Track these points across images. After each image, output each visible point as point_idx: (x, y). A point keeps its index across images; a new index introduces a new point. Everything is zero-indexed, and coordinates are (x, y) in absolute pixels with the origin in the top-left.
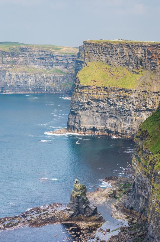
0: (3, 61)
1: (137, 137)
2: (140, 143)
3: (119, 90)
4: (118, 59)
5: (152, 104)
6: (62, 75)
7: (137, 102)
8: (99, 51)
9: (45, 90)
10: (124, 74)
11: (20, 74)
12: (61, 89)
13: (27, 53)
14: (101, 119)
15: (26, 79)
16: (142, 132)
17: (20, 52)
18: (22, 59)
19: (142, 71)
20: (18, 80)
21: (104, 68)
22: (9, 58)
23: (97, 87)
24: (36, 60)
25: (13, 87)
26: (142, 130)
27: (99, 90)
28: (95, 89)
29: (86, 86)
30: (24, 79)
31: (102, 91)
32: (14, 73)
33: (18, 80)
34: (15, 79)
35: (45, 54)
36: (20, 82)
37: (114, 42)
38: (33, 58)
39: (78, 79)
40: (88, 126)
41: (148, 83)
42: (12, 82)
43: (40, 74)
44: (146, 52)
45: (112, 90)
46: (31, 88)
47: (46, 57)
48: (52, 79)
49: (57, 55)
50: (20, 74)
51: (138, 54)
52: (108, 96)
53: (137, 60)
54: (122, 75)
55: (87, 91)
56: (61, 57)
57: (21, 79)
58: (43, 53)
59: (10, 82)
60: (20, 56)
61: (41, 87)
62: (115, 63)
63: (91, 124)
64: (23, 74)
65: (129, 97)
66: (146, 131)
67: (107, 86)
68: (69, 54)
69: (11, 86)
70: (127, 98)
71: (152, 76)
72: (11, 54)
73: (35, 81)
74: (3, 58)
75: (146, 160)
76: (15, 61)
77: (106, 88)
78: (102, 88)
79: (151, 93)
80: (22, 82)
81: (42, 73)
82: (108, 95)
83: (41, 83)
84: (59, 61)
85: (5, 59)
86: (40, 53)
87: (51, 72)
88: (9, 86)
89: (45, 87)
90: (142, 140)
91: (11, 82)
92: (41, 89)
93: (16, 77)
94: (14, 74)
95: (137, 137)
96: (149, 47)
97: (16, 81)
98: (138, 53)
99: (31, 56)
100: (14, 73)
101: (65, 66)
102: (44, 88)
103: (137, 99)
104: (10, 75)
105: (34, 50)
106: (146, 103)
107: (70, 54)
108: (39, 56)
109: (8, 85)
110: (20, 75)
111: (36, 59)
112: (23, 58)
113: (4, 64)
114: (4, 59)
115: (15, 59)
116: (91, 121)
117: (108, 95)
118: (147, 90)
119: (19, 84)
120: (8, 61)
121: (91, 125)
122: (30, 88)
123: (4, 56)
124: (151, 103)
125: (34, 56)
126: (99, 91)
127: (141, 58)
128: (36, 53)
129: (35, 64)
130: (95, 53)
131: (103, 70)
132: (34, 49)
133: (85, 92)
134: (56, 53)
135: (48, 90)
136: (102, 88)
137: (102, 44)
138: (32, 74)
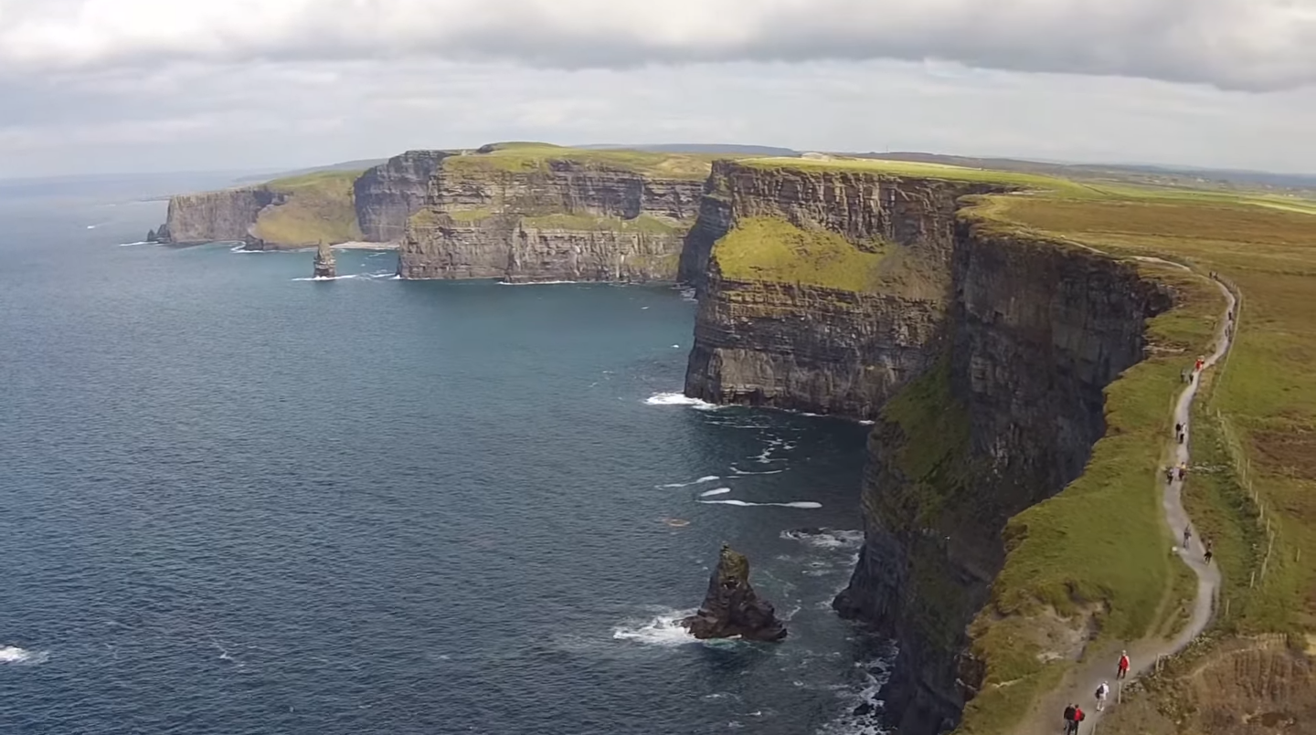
0: (504, 198)
1: (876, 437)
2: (880, 455)
3: (824, 293)
4: (820, 212)
5: (907, 333)
6: (663, 235)
7: (869, 328)
8: (770, 190)
9: (618, 276)
10: (837, 252)
11: (548, 233)
12: (659, 271)
13: (570, 176)
14: (776, 369)
15: (566, 246)
16: (887, 425)
17: (550, 173)
18: (556, 191)
19: (881, 245)
20: (546, 249)
21: (783, 235)
22: (522, 190)
23: (765, 285)
24: (592, 193)
26: (888, 420)
27: (772, 294)
28: (759, 288)
29: (736, 282)
30: (560, 245)
31: (777, 294)
32: (535, 230)
33: (546, 249)
34: (538, 247)
35: (616, 178)
36: (548, 253)
37: (810, 167)
38: (583, 189)
39: (716, 263)
40: (742, 387)
41: (897, 278)
42: (529, 255)
43: (604, 232)
44: (893, 198)
45: (804, 293)
46: (578, 270)
47: (620, 185)
48: (636, 247)
49: (650, 180)
51: (872, 202)
52: (794, 309)
53: (870, 216)
54: (832, 254)
55: (738, 295)
56: (660, 187)
57: (553, 245)
58: (612, 175)
59: (524, 255)
60: (551, 182)
61: (606, 266)
62: (813, 221)
63: (749, 383)
64: (559, 232)
65: (848, 313)
66: (897, 423)
67: (793, 282)
68: (683, 177)
69: (525, 264)
70: (845, 317)
71: (908, 261)
72: (526, 179)
73: (589, 250)
74: (504, 189)
75: (894, 496)
76: (537, 198)
77: (787, 289)
78: (778, 287)
79: (908, 304)
80: (553, 253)
81: (609, 228)
82: (795, 305)
83: (607, 255)
84: (657, 197)
86: (604, 175)
87: (635, 225)
88: (519, 264)
89: (617, 268)
90: (887, 445)
91: (527, 254)
92: (606, 272)
93: (538, 240)
94: (532, 232)
95: (876, 437)
96: (899, 183)
97: (539, 250)
98: (873, 197)
99: (581, 182)
100: (535, 230)
101: (671, 210)
102: (615, 270)
103: (870, 319)
104: (523, 235)
105: (588, 168)
106: (893, 330)
107: (685, 176)
108: (601, 184)
109: (518, 262)
111: (594, 190)
112: (559, 187)
113: (507, 206)
114: (506, 191)
115: (535, 192)
116: (749, 374)
117: (795, 305)
118: (896, 296)
119: (546, 260)
120: (517, 198)
121: (748, 386)
122: (576, 271)
124: (904, 330)
125: (589, 183)
126: (769, 295)
127: (880, 212)
128: (593, 174)
129: (588, 205)
130: (760, 195)
131: (783, 239)
132: (587, 165)
133: (733, 298)
134: (648, 175)
135: (625, 274)
136: (778, 287)
137: (778, 171)
138: (583, 234)
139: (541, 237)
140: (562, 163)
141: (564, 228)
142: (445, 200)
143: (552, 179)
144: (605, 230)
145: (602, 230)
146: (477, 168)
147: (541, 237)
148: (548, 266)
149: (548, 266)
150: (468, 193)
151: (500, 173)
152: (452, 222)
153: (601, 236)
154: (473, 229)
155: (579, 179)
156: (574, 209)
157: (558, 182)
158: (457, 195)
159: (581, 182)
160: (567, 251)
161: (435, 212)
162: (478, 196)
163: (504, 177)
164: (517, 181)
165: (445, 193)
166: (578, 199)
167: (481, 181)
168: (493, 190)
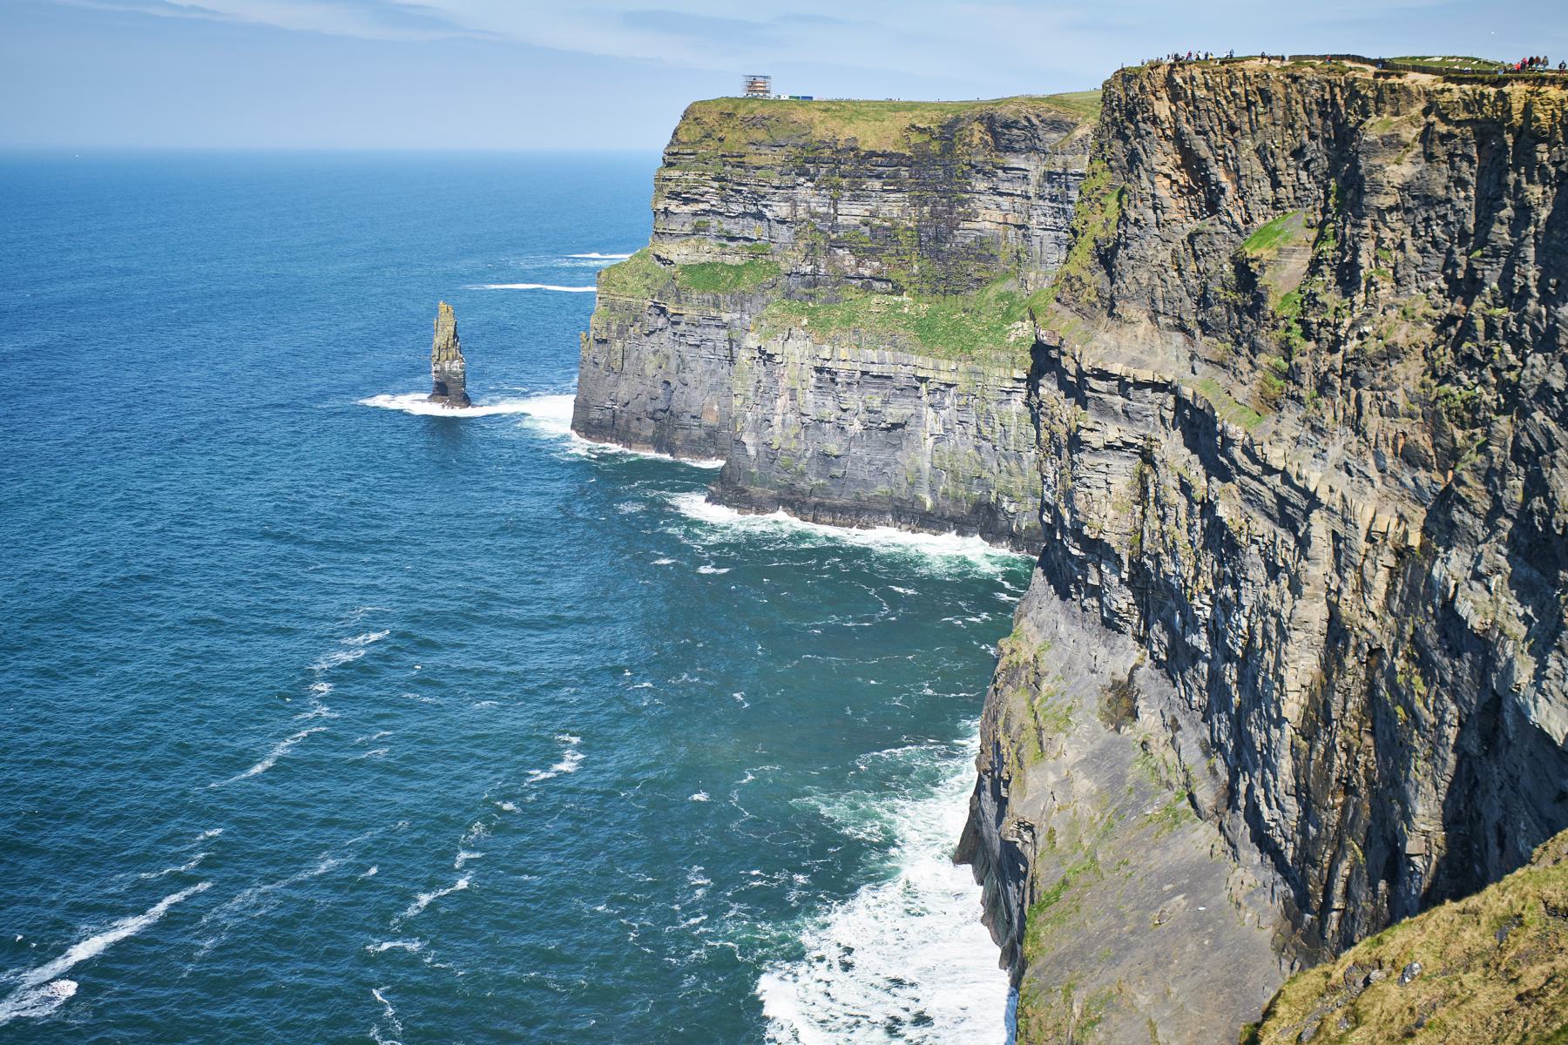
11: (845, 358)
13: (1034, 167)
15: (895, 411)
50: (843, 353)
60: (981, 185)
74: (835, 201)
88: (752, 451)
112: (1005, 202)
114: (843, 208)
123: (845, 182)
139: (819, 370)
142: (674, 226)
146: (760, 135)
147: (819, 370)
150: (737, 208)
151: (828, 152)
157: (1004, 187)
158: (706, 213)
161: (659, 258)
162: (760, 216)
163: (847, 167)
164: (879, 177)
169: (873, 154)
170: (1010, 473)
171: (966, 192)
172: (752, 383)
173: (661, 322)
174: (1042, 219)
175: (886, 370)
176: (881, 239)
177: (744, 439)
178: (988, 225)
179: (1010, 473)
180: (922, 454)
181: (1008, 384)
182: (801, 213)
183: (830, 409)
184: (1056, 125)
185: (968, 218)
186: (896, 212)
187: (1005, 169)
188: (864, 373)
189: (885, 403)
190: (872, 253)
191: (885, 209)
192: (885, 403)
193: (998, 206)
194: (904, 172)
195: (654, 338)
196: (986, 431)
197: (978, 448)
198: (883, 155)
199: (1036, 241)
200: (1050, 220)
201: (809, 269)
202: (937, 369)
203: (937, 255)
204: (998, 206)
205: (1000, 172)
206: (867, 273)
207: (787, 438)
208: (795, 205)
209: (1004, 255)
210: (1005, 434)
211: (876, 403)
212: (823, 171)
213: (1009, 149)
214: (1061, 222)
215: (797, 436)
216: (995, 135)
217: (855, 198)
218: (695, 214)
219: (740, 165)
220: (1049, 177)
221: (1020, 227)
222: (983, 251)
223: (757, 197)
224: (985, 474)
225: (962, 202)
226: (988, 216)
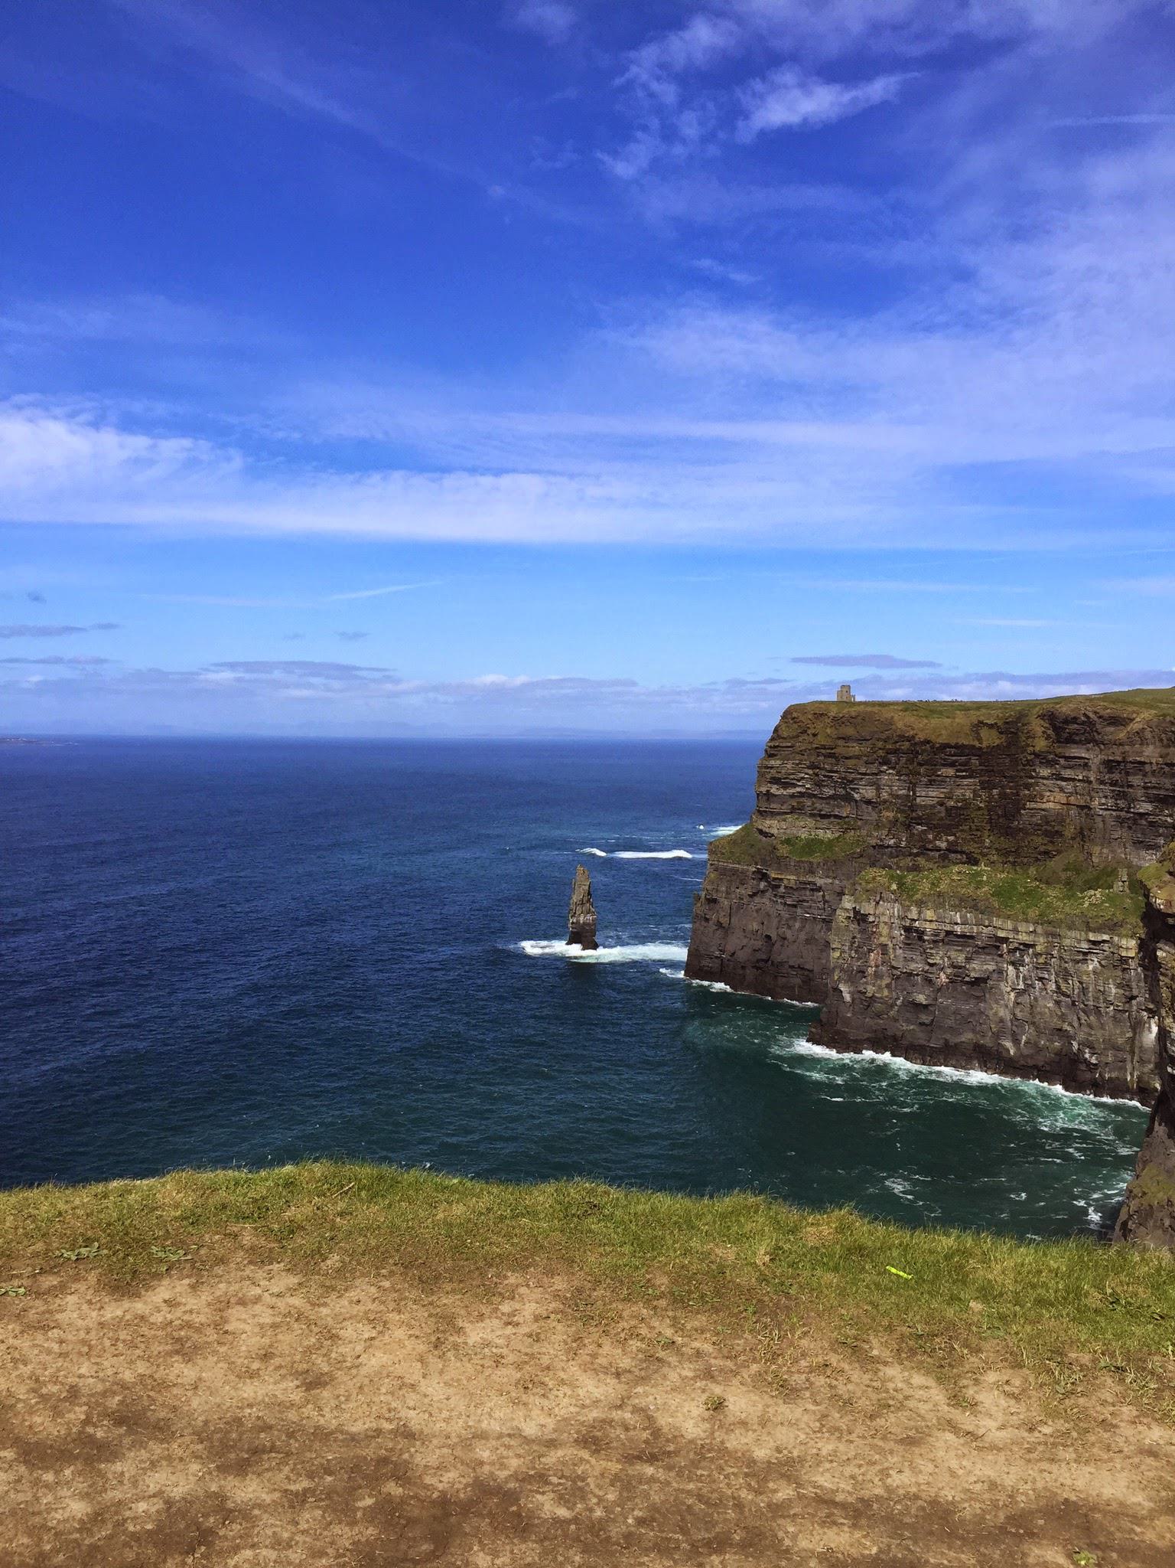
0: (913, 808)
11: (929, 920)
13: (1095, 757)
15: (978, 967)
24: (1145, 807)
25: (878, 1015)
36: (929, 982)
38: (1122, 794)
43: (1092, 937)
50: (929, 914)
60: (1045, 772)
61: (1092, 1048)
64: (958, 920)
74: (913, 786)
81: (1112, 927)
85: (928, 796)
88: (847, 997)
94: (887, 914)
99: (1116, 776)
104: (860, 918)
110: (929, 927)
112: (1069, 787)
114: (920, 792)
122: (1008, 1044)
123: (922, 770)
129: (1139, 844)
140: (1075, 720)
141: (975, 908)
143: (1050, 764)
144: (1098, 930)
145: (1089, 929)
146: (850, 731)
147: (908, 930)
148: (925, 1018)
149: (925, 1018)
152: (780, 862)
153: (1085, 946)
154: (820, 882)
155: (1110, 765)
156: (1096, 850)
157: (1067, 773)
158: (802, 795)
159: (1116, 776)
160: (985, 980)
161: (761, 832)
162: (848, 798)
164: (952, 765)
165: (774, 790)
166: (1111, 822)
167: (850, 763)
168: (892, 784)
169: (948, 746)
170: (1090, 1026)
171: (1032, 777)
172: (848, 937)
173: (762, 885)
174: (1103, 801)
175: (966, 929)
176: (955, 817)
177: (842, 987)
178: (1051, 805)
179: (1090, 1026)
180: (1003, 1005)
181: (1085, 946)
182: (885, 795)
183: (917, 966)
184: (1116, 721)
185: (1032, 799)
186: (969, 794)
187: (1067, 758)
188: (948, 933)
189: (968, 959)
190: (948, 829)
191: (958, 792)
192: (968, 959)
193: (1062, 790)
194: (975, 761)
195: (757, 899)
196: (1063, 986)
197: (1058, 1003)
198: (957, 746)
199: (1098, 820)
200: (1110, 802)
201: (892, 842)
202: (1016, 931)
203: (1008, 832)
204: (1062, 790)
205: (1062, 761)
206: (944, 845)
207: (880, 988)
208: (878, 789)
209: (1069, 831)
210: (1084, 990)
211: (961, 958)
212: (903, 760)
213: (1070, 740)
214: (1121, 803)
215: (888, 986)
216: (1055, 729)
217: (931, 783)
218: (792, 796)
219: (831, 756)
220: (1110, 765)
221: (1082, 807)
222: (1051, 829)
223: (846, 782)
224: (1066, 1027)
225: (1027, 786)
226: (1051, 799)
